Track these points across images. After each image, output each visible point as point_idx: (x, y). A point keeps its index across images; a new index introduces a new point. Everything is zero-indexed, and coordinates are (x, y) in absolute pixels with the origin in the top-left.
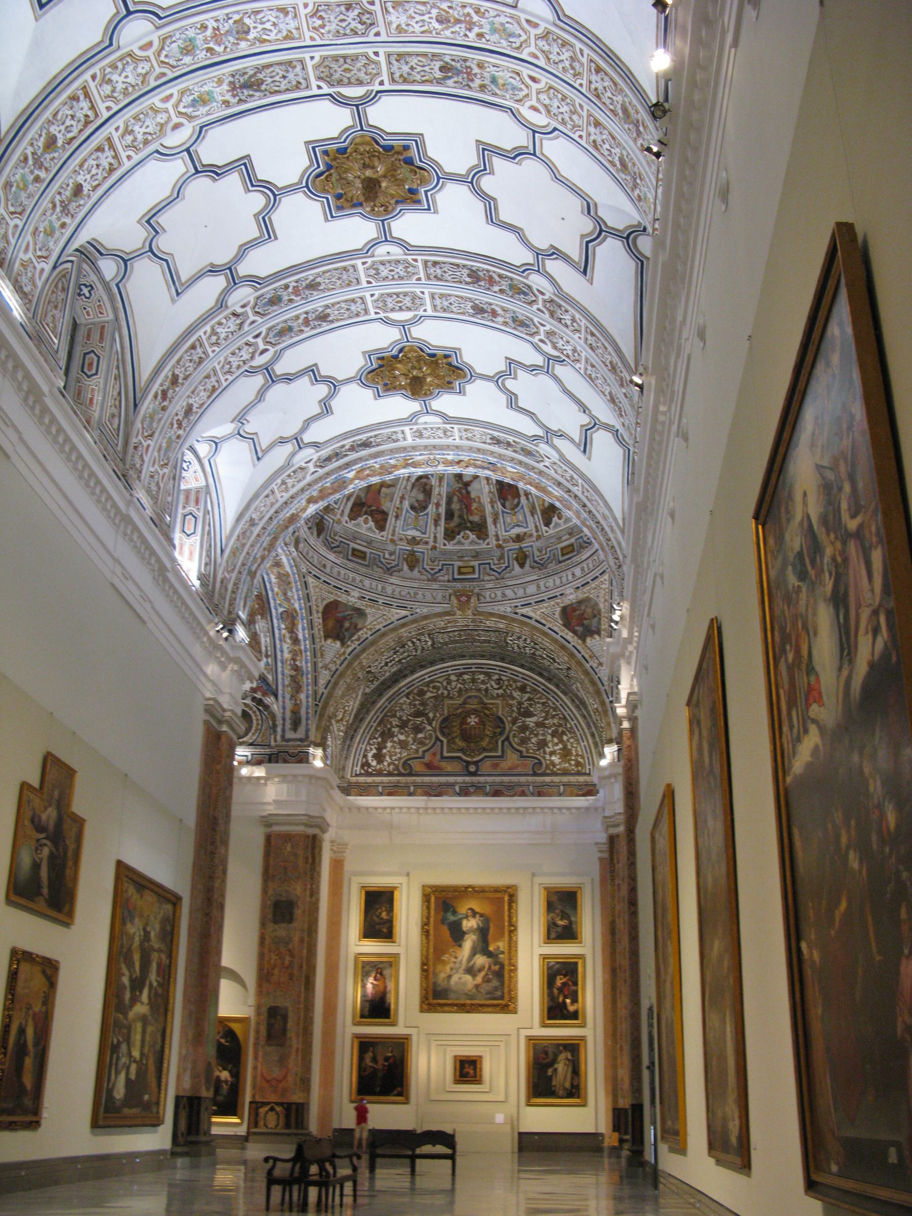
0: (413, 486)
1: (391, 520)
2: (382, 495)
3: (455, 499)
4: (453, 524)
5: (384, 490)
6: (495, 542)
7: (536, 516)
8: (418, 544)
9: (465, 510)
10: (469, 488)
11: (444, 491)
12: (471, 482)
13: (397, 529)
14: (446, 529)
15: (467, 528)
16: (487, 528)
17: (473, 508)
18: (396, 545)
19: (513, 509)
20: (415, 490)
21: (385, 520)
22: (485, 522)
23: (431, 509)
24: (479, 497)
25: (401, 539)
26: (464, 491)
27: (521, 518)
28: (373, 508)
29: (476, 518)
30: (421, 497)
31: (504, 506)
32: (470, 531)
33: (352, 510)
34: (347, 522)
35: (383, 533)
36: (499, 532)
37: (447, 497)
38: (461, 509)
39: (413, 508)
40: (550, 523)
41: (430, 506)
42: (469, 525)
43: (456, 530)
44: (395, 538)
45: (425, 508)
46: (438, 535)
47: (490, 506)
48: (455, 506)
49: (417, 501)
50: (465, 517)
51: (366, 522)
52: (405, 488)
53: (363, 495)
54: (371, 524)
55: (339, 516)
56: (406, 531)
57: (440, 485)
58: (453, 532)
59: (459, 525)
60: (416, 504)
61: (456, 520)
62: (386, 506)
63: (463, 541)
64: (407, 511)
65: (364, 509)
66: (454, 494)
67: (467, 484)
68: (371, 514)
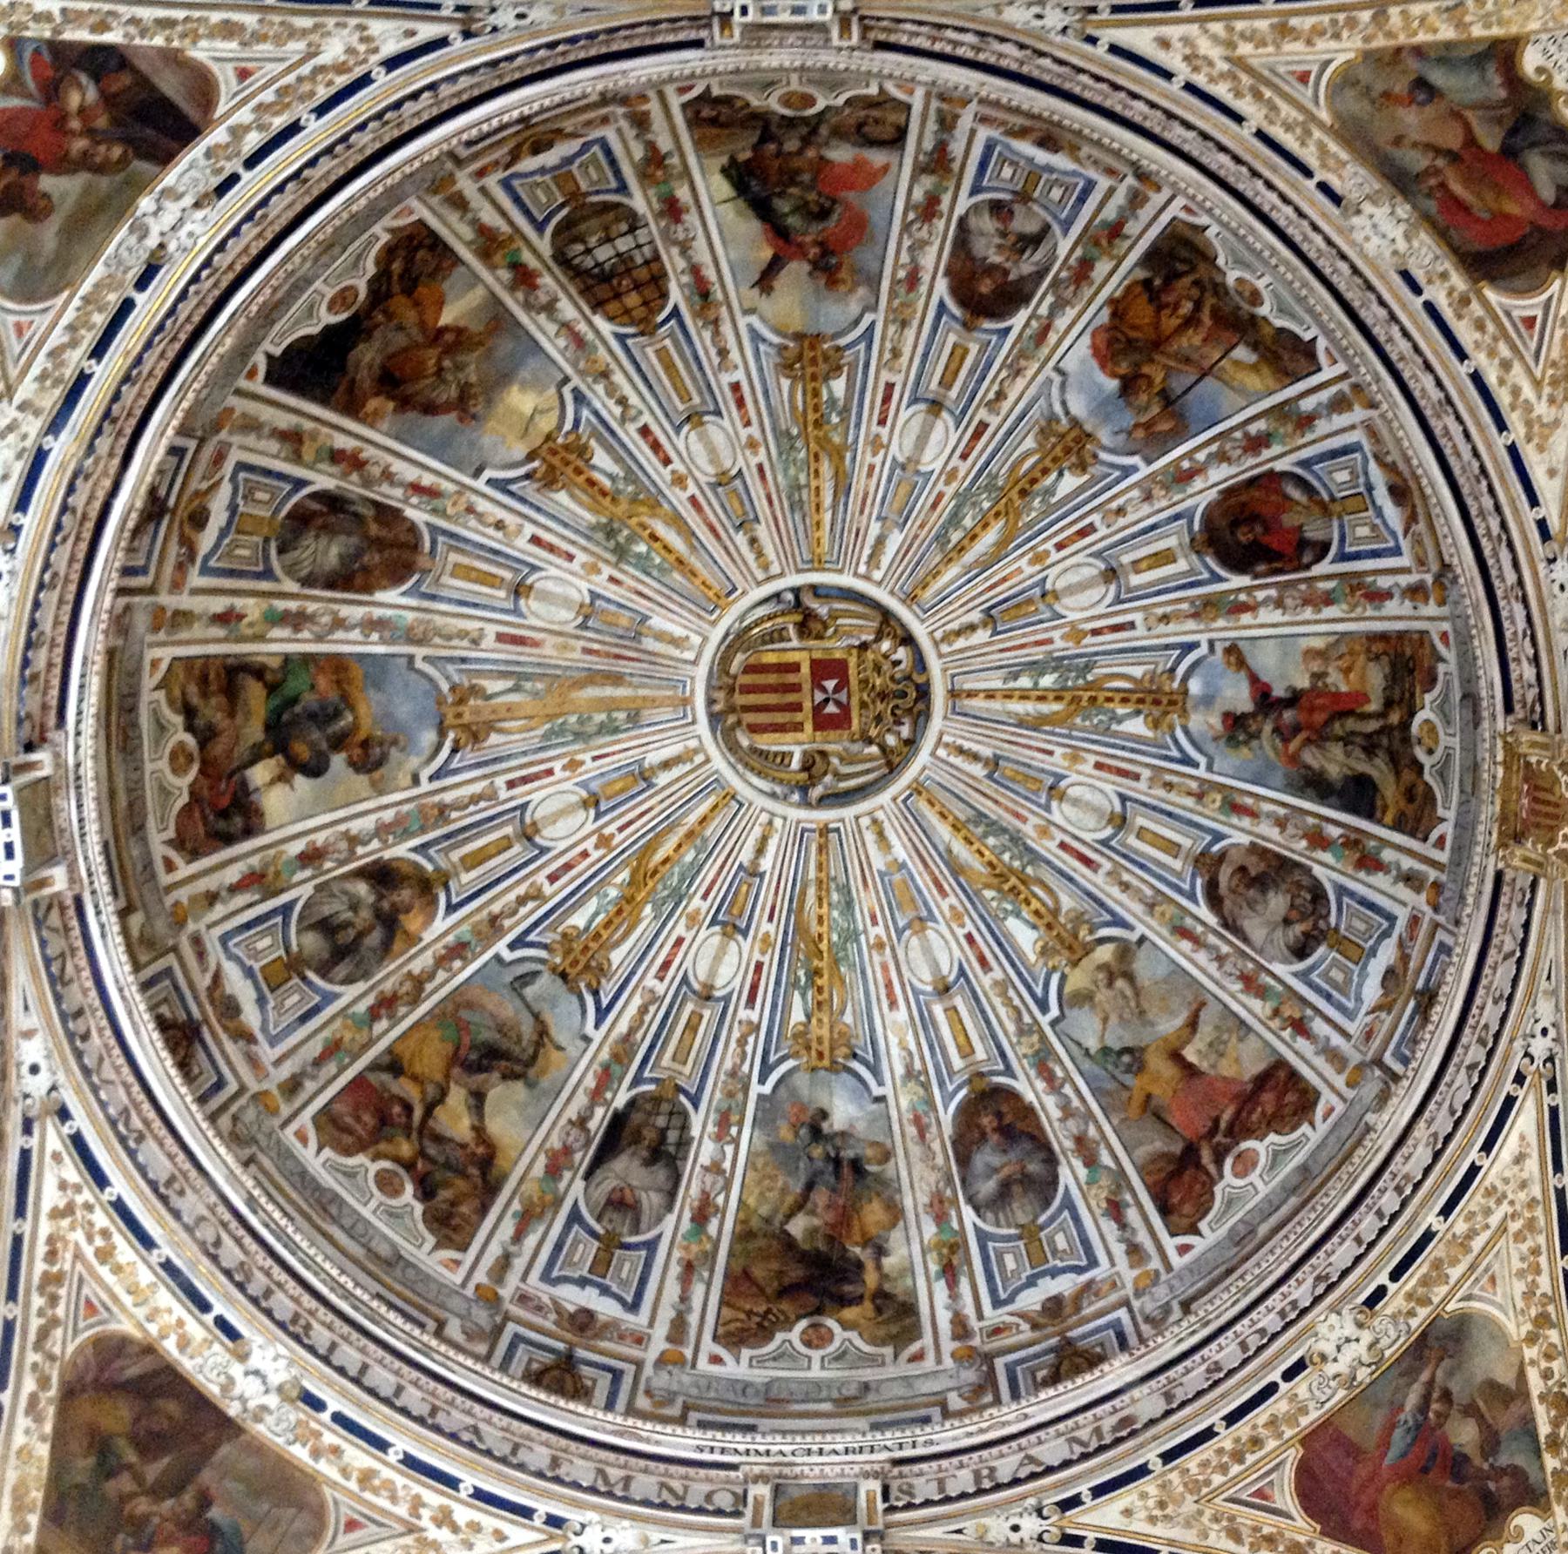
0: (1231, 925)
1: (1304, 1058)
2: (1204, 1066)
3: (1311, 757)
4: (1390, 791)
5: (1190, 1054)
6: (1431, 609)
7: (1307, 405)
8: (1405, 958)
9: (1351, 724)
10: (1279, 691)
11: (1274, 797)
12: (1254, 679)
13: (1337, 1040)
14: (1398, 826)
15: (1405, 725)
16: (1401, 635)
17: (1344, 688)
18: (1378, 1062)
19: (1325, 509)
20: (1256, 928)
21: (1294, 1075)
22: (1383, 637)
23: (1327, 869)
24: (1311, 654)
25: (1369, 1035)
26: (1288, 715)
27: (1342, 476)
28: (1226, 1116)
29: (1375, 679)
30: (1277, 903)
31: (1322, 549)
32: (1412, 714)
33: (1165, 1210)
34: (1183, 1249)
35: (1320, 1110)
36: (1404, 580)
37: (1299, 791)
38: (1346, 740)
39: (1301, 952)
40: (1296, 337)
41: (1318, 871)
42: (1394, 718)
43: (1408, 776)
44: (1355, 1058)
45: (1318, 894)
46: (1407, 863)
47: (1330, 612)
48: (1334, 762)
49: (1287, 922)
50: (1372, 726)
51: (1245, 1164)
52: (1220, 959)
53: (1157, 1144)
54: (1260, 1147)
55: (1129, 1275)
56: (1359, 999)
57: (1253, 814)
58: (1410, 795)
59: (1394, 761)
60: (1298, 929)
61: (1378, 769)
62: (1246, 1063)
63: (1439, 752)
64: (1303, 976)
65: (1206, 1156)
66: (1294, 759)
67: (1265, 700)
68: (1240, 1129)
